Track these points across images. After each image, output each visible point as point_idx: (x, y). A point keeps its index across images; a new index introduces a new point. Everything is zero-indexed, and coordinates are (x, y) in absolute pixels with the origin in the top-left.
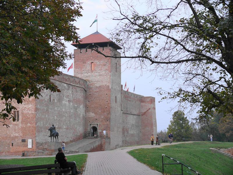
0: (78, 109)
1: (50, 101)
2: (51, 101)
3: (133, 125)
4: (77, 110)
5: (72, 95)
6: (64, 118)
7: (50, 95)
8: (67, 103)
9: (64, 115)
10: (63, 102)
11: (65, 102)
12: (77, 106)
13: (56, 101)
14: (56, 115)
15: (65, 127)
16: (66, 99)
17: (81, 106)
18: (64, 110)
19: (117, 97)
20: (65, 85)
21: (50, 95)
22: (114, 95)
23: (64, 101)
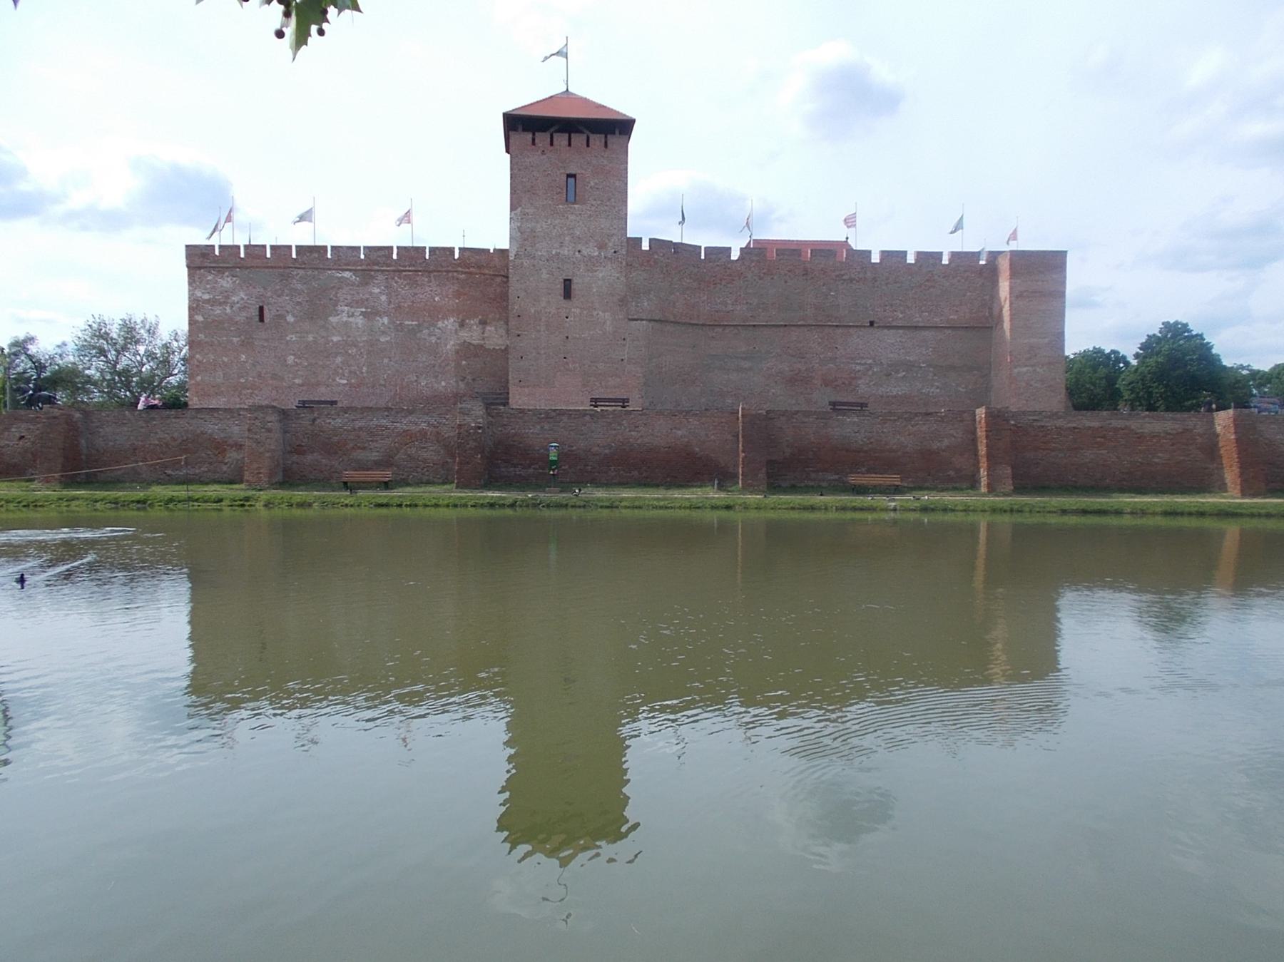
0: (426, 331)
1: (261, 318)
2: (267, 320)
3: (909, 366)
4: (418, 335)
5: (383, 298)
6: (339, 360)
7: (261, 309)
8: (360, 321)
9: (343, 351)
10: (333, 319)
11: (345, 319)
12: (419, 325)
13: (290, 319)
14: (294, 355)
15: (345, 382)
16: (353, 310)
17: (450, 323)
18: (335, 339)
19: (575, 280)
20: (347, 274)
21: (261, 309)
22: (545, 276)
23: (339, 317)
